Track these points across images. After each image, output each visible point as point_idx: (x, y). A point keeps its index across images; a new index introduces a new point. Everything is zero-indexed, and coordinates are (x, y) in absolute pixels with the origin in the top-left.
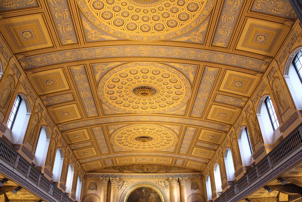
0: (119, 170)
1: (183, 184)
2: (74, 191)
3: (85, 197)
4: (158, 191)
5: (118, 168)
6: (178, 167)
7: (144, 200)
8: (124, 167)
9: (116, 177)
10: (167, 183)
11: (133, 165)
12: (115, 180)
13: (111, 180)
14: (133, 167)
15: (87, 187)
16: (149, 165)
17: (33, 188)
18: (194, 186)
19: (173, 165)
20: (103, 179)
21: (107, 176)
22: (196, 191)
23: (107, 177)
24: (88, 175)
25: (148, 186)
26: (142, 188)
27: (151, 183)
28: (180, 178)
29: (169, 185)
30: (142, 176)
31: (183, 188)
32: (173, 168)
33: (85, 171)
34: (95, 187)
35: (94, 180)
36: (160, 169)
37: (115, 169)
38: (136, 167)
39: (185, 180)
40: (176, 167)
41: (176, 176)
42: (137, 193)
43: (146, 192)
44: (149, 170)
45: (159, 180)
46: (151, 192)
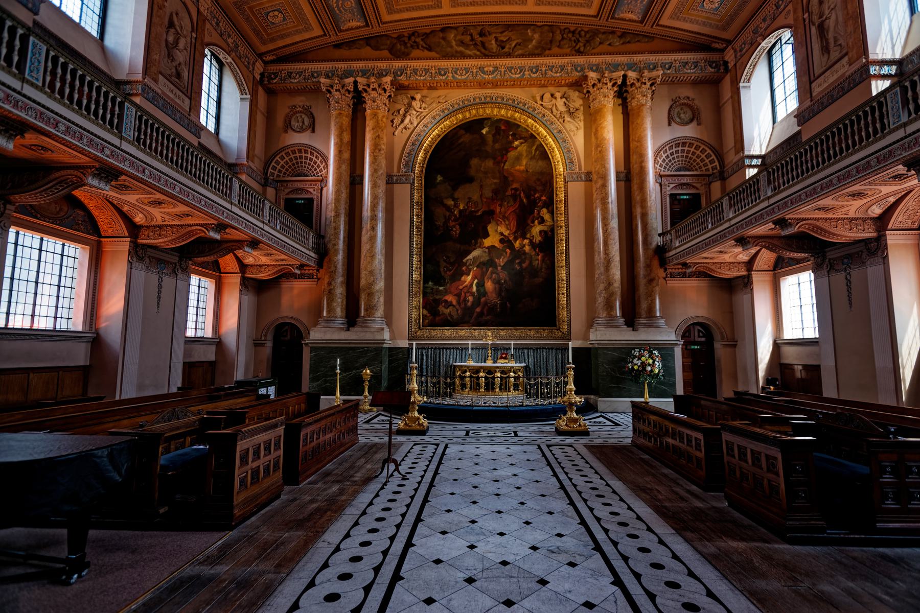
0: (390, 52)
1: (642, 98)
2: (183, 96)
3: (275, 155)
4: (541, 129)
5: (388, 42)
6: (623, 35)
7: (489, 163)
8: (409, 38)
9: (380, 75)
10: (577, 101)
11: (443, 30)
12: (376, 86)
13: (360, 87)
14: (444, 38)
15: (280, 122)
16: (509, 27)
17: (181, 188)
18: (679, 114)
19: (605, 14)
20: (332, 87)
21: (348, 73)
22: (688, 131)
23: (347, 78)
24: (275, 74)
25: (503, 112)
26: (478, 123)
27: (514, 101)
28: (632, 75)
29: (582, 108)
30: (481, 69)
31: (639, 116)
32: (603, 37)
33: (260, 56)
34: (306, 123)
35: (303, 98)
36: (551, 42)
37: (376, 48)
38: (455, 36)
39: (648, 84)
40: (613, 33)
41: (616, 67)
42: (460, 141)
43: (494, 136)
44: (507, 46)
45: (544, 89)
46: (515, 138)
